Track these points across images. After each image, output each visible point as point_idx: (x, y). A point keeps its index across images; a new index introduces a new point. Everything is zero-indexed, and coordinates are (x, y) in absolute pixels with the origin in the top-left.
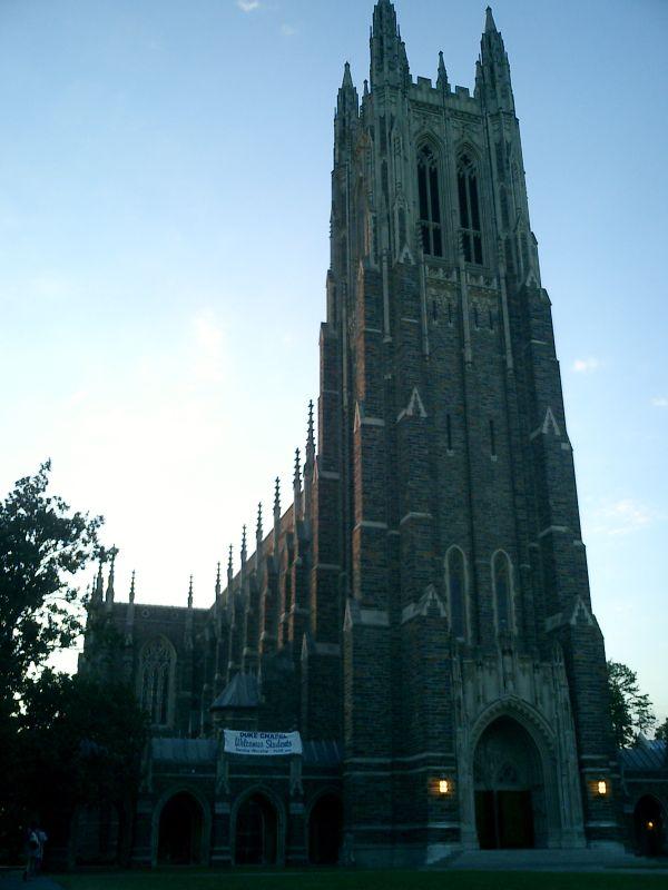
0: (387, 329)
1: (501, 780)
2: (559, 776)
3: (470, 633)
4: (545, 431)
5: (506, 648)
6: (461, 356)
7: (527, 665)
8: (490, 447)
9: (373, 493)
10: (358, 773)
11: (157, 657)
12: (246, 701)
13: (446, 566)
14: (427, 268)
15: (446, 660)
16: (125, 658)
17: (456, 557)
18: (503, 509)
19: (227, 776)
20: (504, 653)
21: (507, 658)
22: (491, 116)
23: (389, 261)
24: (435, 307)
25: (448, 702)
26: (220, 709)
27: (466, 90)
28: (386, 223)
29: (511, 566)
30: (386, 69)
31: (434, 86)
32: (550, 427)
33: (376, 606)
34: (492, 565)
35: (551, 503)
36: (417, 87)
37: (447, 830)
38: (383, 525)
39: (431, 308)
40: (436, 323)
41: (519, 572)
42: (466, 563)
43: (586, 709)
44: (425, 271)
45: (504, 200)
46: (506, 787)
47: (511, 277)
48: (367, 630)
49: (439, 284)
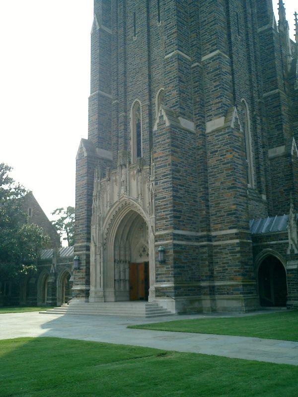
13: (131, 116)
43: (160, 196)
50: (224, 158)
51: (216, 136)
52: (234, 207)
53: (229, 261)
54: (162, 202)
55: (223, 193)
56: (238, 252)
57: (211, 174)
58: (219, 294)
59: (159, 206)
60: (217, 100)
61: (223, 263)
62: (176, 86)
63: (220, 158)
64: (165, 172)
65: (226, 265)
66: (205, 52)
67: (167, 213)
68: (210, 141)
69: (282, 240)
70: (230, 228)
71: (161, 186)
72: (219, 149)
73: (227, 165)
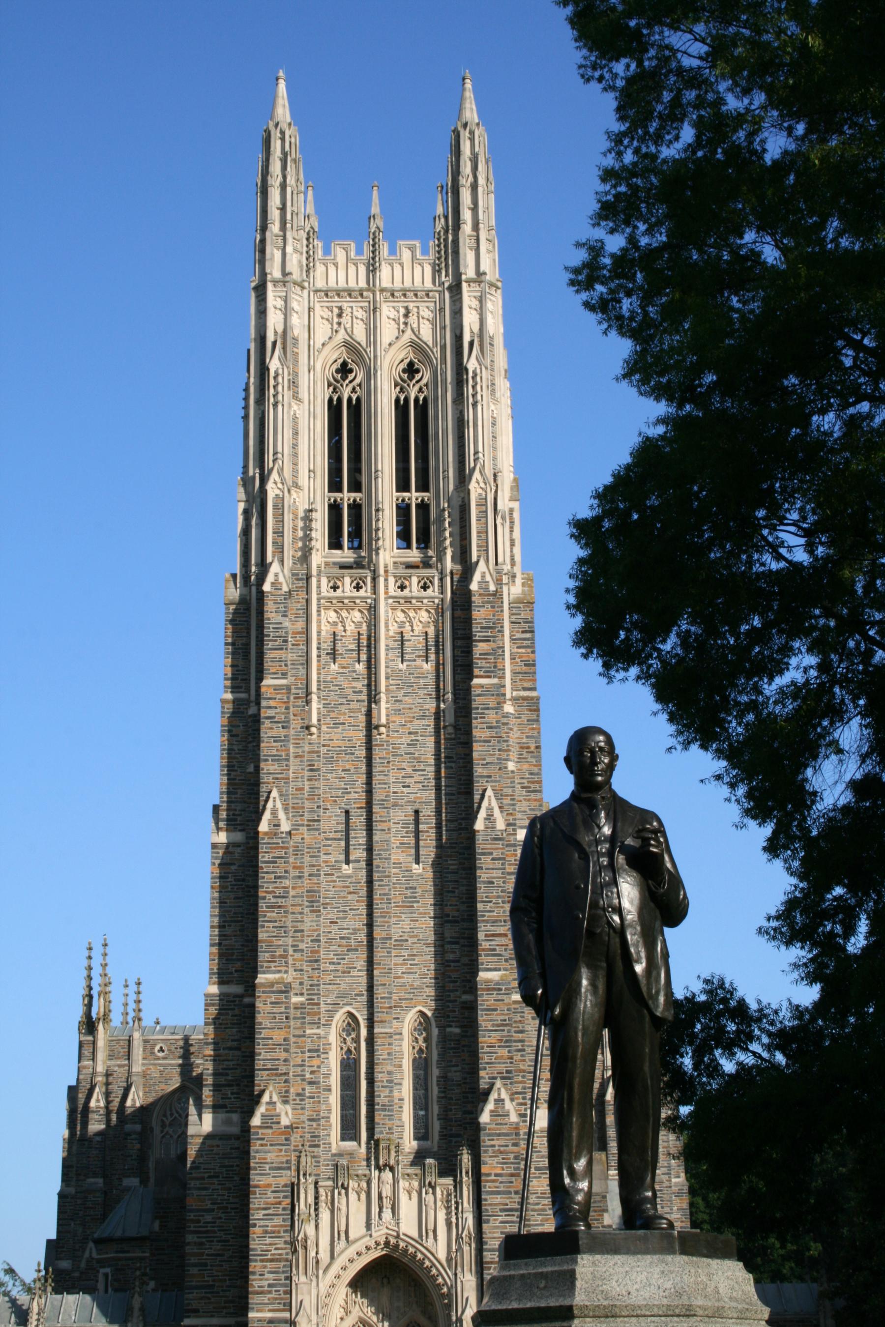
8: (413, 851)
12: (132, 1232)
14: (324, 581)
15: (285, 1186)
25: (286, 1242)
32: (489, 817)
34: (406, 1032)
39: (327, 646)
40: (334, 667)
44: (321, 587)
57: (536, 1207)
62: (507, 1041)
71: (497, 1227)
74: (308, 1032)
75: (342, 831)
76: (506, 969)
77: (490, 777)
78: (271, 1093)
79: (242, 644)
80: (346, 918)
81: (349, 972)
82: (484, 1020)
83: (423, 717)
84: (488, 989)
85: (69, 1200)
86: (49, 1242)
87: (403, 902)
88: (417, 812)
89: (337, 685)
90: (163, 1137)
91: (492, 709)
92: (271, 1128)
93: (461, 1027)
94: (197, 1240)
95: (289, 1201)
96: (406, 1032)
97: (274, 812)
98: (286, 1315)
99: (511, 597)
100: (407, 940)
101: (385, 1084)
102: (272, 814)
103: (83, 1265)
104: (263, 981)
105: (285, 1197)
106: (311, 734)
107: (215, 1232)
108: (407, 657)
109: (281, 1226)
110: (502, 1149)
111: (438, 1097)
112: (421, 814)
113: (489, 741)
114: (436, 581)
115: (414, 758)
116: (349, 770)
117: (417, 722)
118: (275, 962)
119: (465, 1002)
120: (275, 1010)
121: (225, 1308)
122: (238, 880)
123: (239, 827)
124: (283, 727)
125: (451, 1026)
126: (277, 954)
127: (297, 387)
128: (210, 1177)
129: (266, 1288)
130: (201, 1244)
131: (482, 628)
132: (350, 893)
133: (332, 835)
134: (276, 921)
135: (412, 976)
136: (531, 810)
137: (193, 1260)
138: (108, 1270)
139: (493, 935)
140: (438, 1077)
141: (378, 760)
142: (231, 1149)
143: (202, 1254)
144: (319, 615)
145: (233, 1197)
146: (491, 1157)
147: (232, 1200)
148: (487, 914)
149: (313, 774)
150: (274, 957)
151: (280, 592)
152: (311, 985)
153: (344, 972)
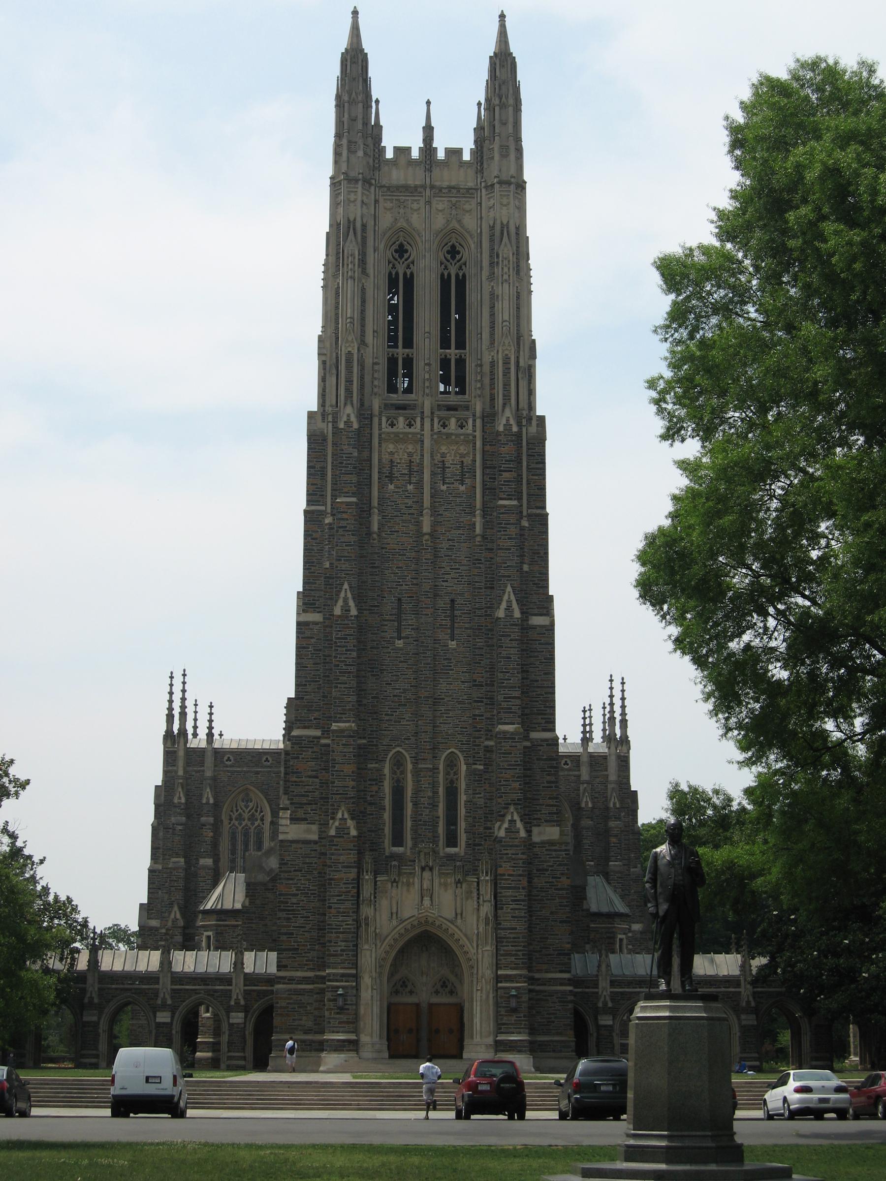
0: (329, 510)
1: (437, 992)
2: (475, 990)
3: (409, 843)
4: (501, 613)
5: (423, 864)
6: (419, 524)
7: (449, 880)
8: (449, 631)
9: (306, 697)
10: (281, 986)
11: (246, 816)
12: (228, 905)
13: (386, 771)
14: (384, 419)
15: (353, 880)
16: (203, 819)
17: (398, 763)
18: (460, 702)
19: (169, 987)
20: (423, 869)
21: (427, 874)
22: (486, 187)
23: (335, 422)
24: (392, 467)
25: (353, 920)
26: (206, 912)
27: (458, 152)
28: (334, 371)
29: (464, 768)
30: (345, 153)
31: (415, 154)
32: (509, 608)
33: (305, 819)
34: (441, 767)
35: (501, 698)
36: (393, 162)
37: (344, 1041)
38: (318, 733)
39: (386, 470)
40: (391, 487)
41: (471, 773)
42: (410, 766)
44: (380, 426)
45: (492, 307)
46: (435, 1000)
47: (489, 417)
48: (294, 845)
49: (398, 438)
50: (557, 882)
51: (547, 850)
52: (569, 946)
53: (558, 1012)
54: (510, 933)
55: (552, 926)
56: (571, 1002)
58: (541, 1052)
59: (504, 938)
60: (551, 802)
61: (547, 1014)
62: (518, 777)
63: (551, 880)
64: (516, 897)
65: (552, 1016)
66: (533, 726)
67: (517, 948)
68: (537, 855)
69: (588, 988)
70: (561, 972)
72: (550, 868)
73: (561, 892)
74: (370, 766)
75: (395, 615)
76: (518, 724)
77: (509, 576)
78: (343, 812)
79: (320, 467)
80: (398, 681)
81: (400, 722)
82: (502, 761)
83: (458, 528)
84: (506, 738)
85: (157, 874)
86: (141, 905)
87: (442, 669)
88: (453, 601)
89: (393, 502)
90: (230, 828)
91: (512, 524)
92: (343, 837)
93: (485, 765)
94: (287, 916)
95: (355, 890)
96: (441, 767)
97: (346, 600)
98: (354, 971)
99: (529, 435)
100: (443, 699)
101: (426, 805)
102: (344, 601)
103: (170, 924)
104: (335, 728)
105: (353, 887)
106: (374, 540)
107: (298, 910)
108: (447, 480)
109: (350, 908)
110: (513, 856)
111: (466, 816)
112: (456, 603)
113: (510, 549)
114: (470, 422)
115: (451, 559)
116: (401, 568)
117: (455, 531)
118: (346, 714)
119: (486, 747)
120: (345, 750)
121: (306, 965)
122: (317, 650)
123: (318, 610)
124: (353, 535)
125: (476, 764)
126: (348, 708)
127: (365, 264)
128: (295, 871)
129: (339, 952)
130: (289, 919)
131: (506, 461)
132: (401, 662)
133: (387, 617)
134: (346, 683)
135: (447, 726)
136: (539, 601)
137: (284, 930)
138: (210, 933)
139: (509, 698)
140: (465, 801)
141: (424, 561)
142: (311, 850)
143: (290, 926)
144: (380, 446)
145: (313, 886)
146: (505, 862)
147: (311, 888)
148: (505, 682)
149: (374, 570)
150: (345, 710)
151: (351, 429)
152: (371, 731)
153: (395, 722)
